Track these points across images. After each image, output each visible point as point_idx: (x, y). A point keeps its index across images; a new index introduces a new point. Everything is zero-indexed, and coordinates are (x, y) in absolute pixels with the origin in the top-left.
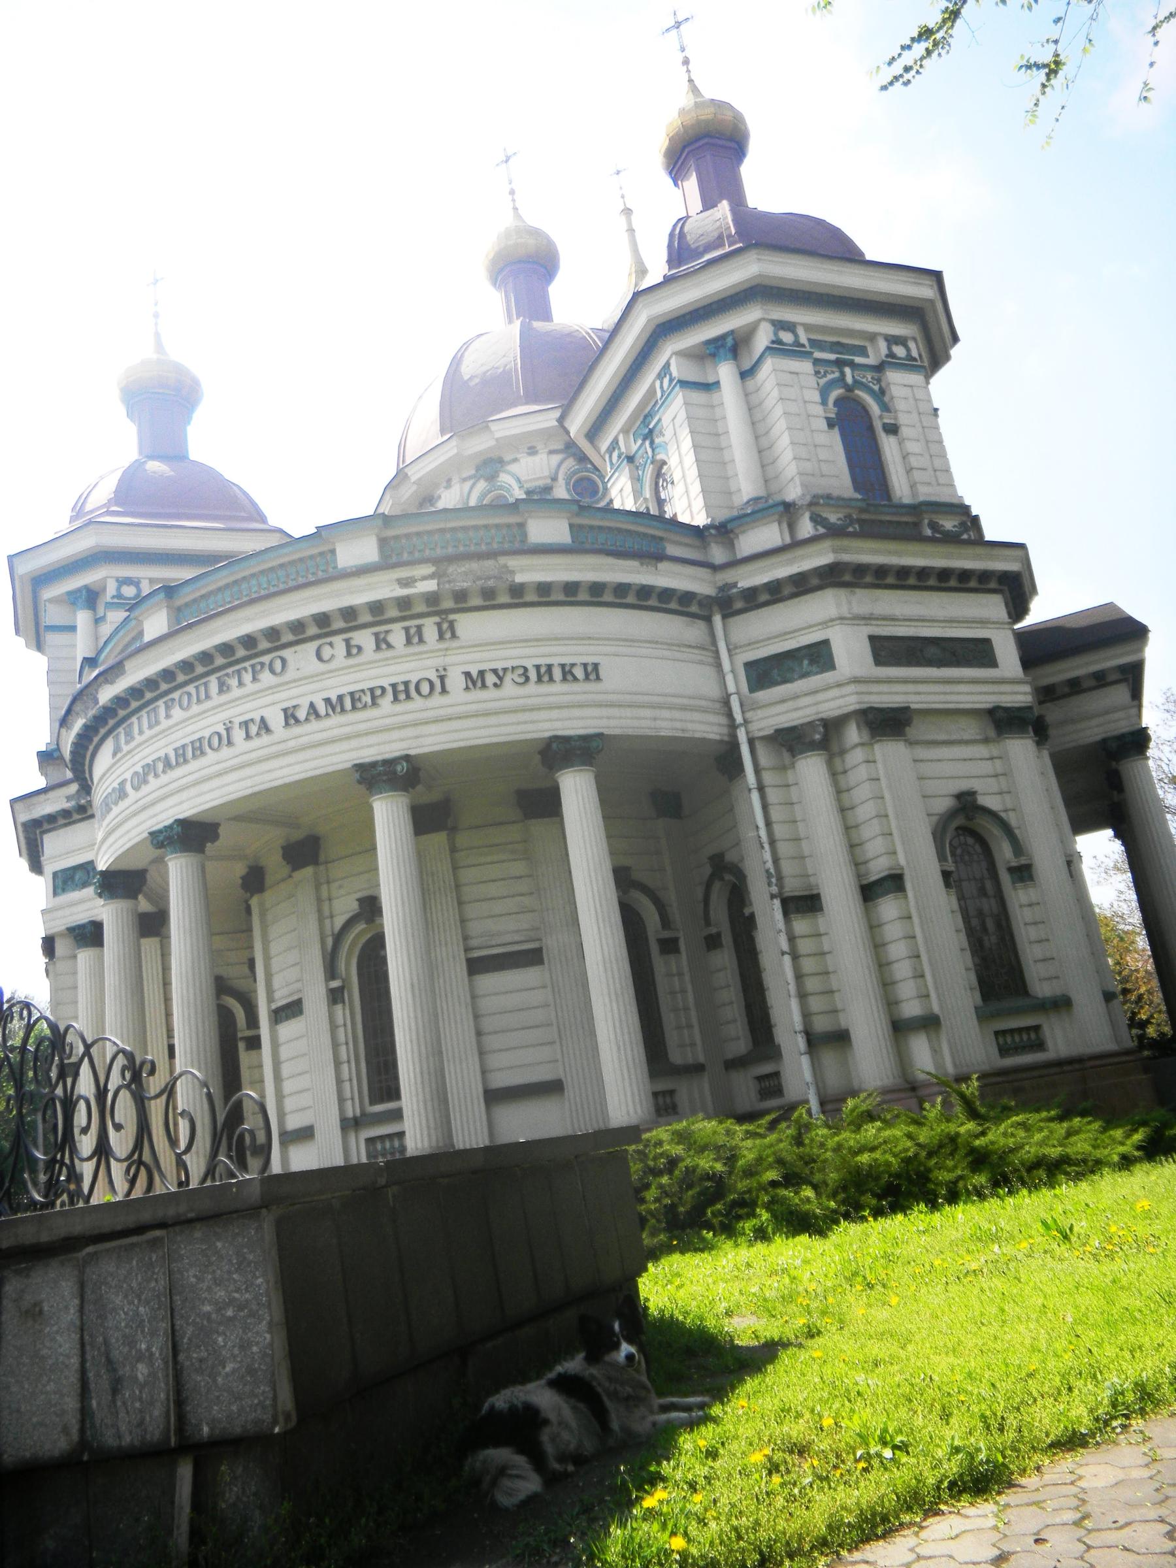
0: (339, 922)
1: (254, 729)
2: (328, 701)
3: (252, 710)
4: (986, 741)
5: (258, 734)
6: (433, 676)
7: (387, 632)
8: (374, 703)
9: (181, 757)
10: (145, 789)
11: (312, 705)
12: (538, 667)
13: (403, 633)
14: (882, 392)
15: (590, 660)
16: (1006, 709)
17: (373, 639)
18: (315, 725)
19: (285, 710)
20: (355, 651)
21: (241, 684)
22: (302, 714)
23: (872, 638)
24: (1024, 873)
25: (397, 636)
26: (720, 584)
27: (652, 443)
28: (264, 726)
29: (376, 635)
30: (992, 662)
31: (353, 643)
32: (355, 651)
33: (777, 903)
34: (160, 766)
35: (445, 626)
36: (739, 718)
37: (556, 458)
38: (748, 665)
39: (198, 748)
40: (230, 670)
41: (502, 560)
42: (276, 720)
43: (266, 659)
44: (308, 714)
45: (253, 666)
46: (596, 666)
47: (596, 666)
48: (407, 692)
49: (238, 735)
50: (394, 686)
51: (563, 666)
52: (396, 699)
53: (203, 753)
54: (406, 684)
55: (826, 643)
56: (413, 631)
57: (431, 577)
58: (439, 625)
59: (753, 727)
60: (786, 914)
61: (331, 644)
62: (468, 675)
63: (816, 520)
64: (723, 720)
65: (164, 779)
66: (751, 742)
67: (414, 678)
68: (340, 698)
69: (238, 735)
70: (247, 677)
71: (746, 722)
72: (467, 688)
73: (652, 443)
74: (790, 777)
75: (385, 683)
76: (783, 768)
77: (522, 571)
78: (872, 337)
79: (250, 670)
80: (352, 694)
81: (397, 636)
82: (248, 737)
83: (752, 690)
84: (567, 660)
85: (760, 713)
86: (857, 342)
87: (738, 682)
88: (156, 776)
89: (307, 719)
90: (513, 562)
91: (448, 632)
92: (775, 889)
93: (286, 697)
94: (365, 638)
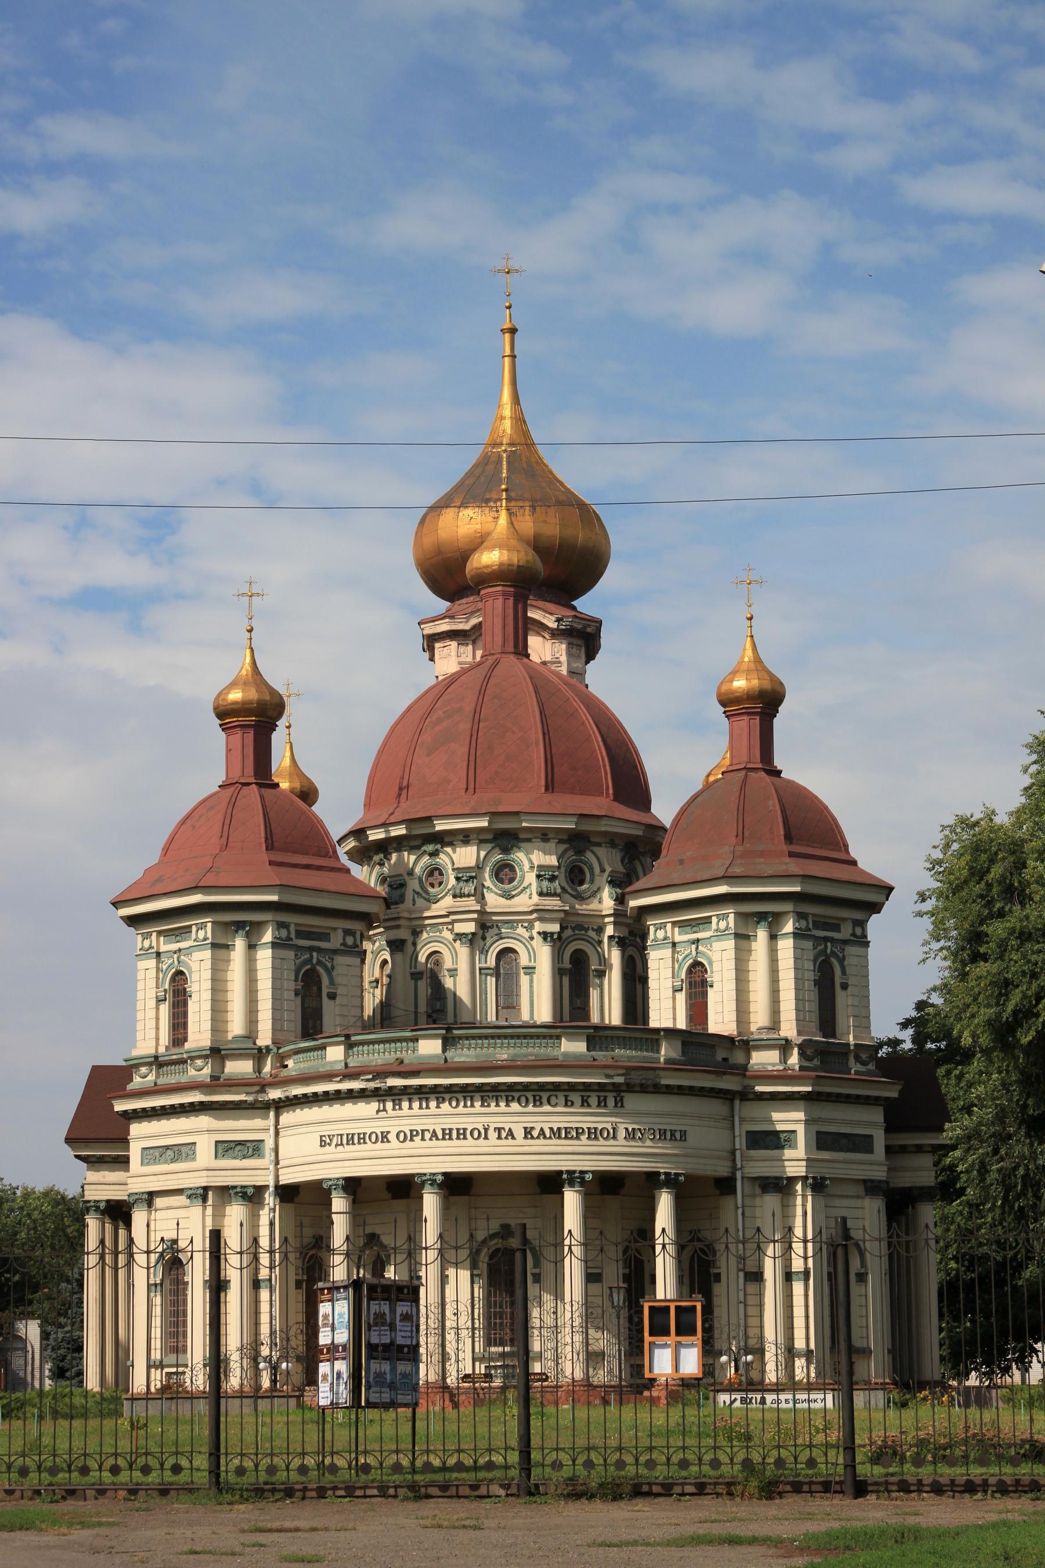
0: (481, 1235)
1: (504, 1135)
2: (551, 1129)
3: (505, 1122)
4: (858, 1197)
5: (506, 1138)
6: (609, 1127)
7: (589, 1097)
8: (578, 1138)
9: (447, 1134)
10: (408, 1143)
11: (542, 1129)
12: (660, 1130)
13: (597, 1098)
14: (844, 958)
15: (683, 1128)
16: (872, 1181)
17: (580, 1098)
18: (542, 1141)
19: (525, 1128)
20: (569, 1103)
21: (497, 1105)
22: (535, 1133)
23: (818, 1133)
24: (862, 1277)
25: (593, 1101)
26: (745, 1084)
27: (697, 948)
28: (511, 1134)
29: (583, 1097)
30: (870, 1150)
31: (569, 1098)
32: (569, 1103)
33: (741, 1274)
34: (427, 1135)
35: (618, 1099)
36: (739, 1166)
37: (563, 847)
38: (748, 1132)
39: (462, 1134)
40: (491, 1094)
41: (658, 1072)
42: (519, 1133)
43: (516, 1095)
44: (539, 1134)
45: (507, 1097)
46: (685, 1131)
47: (685, 1131)
48: (595, 1133)
49: (493, 1135)
50: (589, 1129)
51: (671, 1130)
52: (589, 1138)
53: (465, 1138)
54: (596, 1129)
55: (794, 1132)
56: (602, 1098)
57: (622, 1075)
58: (616, 1098)
59: (746, 1170)
60: (746, 1280)
61: (556, 1096)
62: (627, 1129)
63: (802, 1054)
64: (729, 1164)
65: (428, 1143)
66: (743, 1178)
67: (600, 1126)
68: (559, 1129)
69: (493, 1135)
70: (502, 1104)
71: (742, 1167)
72: (625, 1138)
73: (697, 948)
74: (758, 1201)
75: (585, 1126)
76: (754, 1196)
77: (665, 1077)
78: (844, 920)
79: (504, 1098)
80: (566, 1128)
81: (593, 1101)
82: (499, 1137)
83: (748, 1148)
84: (673, 1128)
85: (751, 1164)
86: (836, 922)
87: (740, 1143)
88: (423, 1139)
89: (538, 1137)
90: (662, 1073)
91: (619, 1103)
92: (741, 1266)
93: (529, 1121)
94: (575, 1097)
